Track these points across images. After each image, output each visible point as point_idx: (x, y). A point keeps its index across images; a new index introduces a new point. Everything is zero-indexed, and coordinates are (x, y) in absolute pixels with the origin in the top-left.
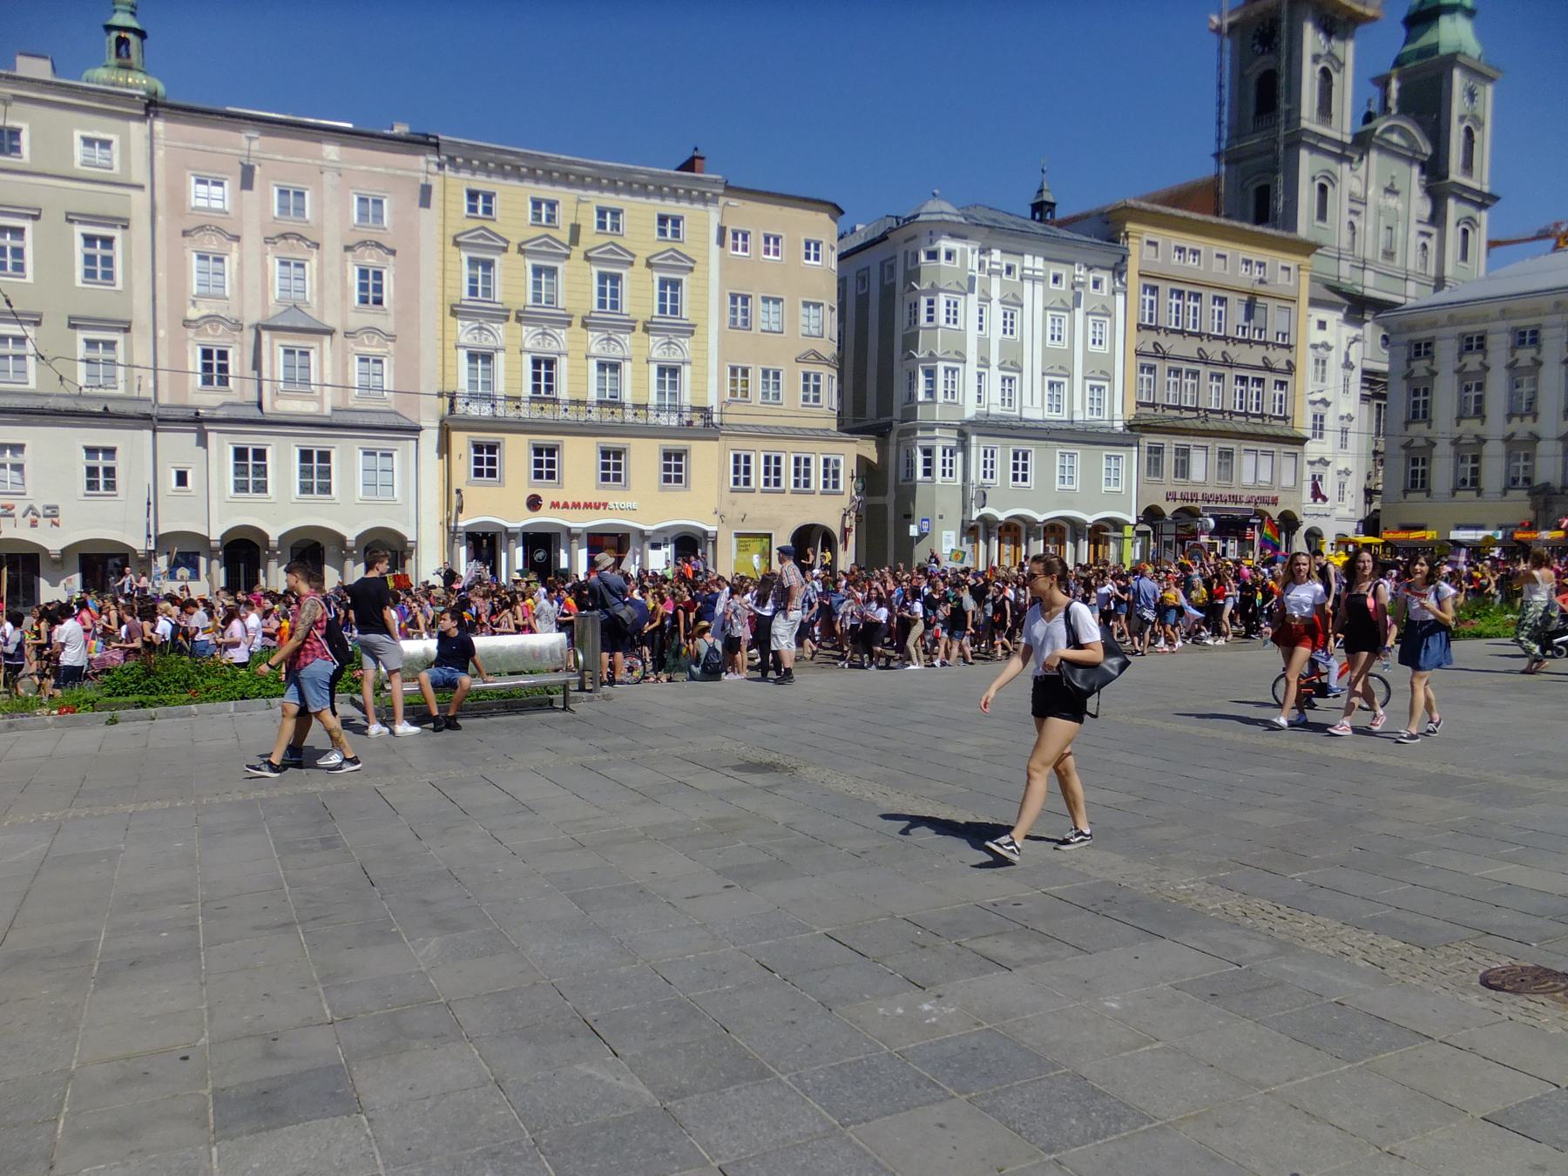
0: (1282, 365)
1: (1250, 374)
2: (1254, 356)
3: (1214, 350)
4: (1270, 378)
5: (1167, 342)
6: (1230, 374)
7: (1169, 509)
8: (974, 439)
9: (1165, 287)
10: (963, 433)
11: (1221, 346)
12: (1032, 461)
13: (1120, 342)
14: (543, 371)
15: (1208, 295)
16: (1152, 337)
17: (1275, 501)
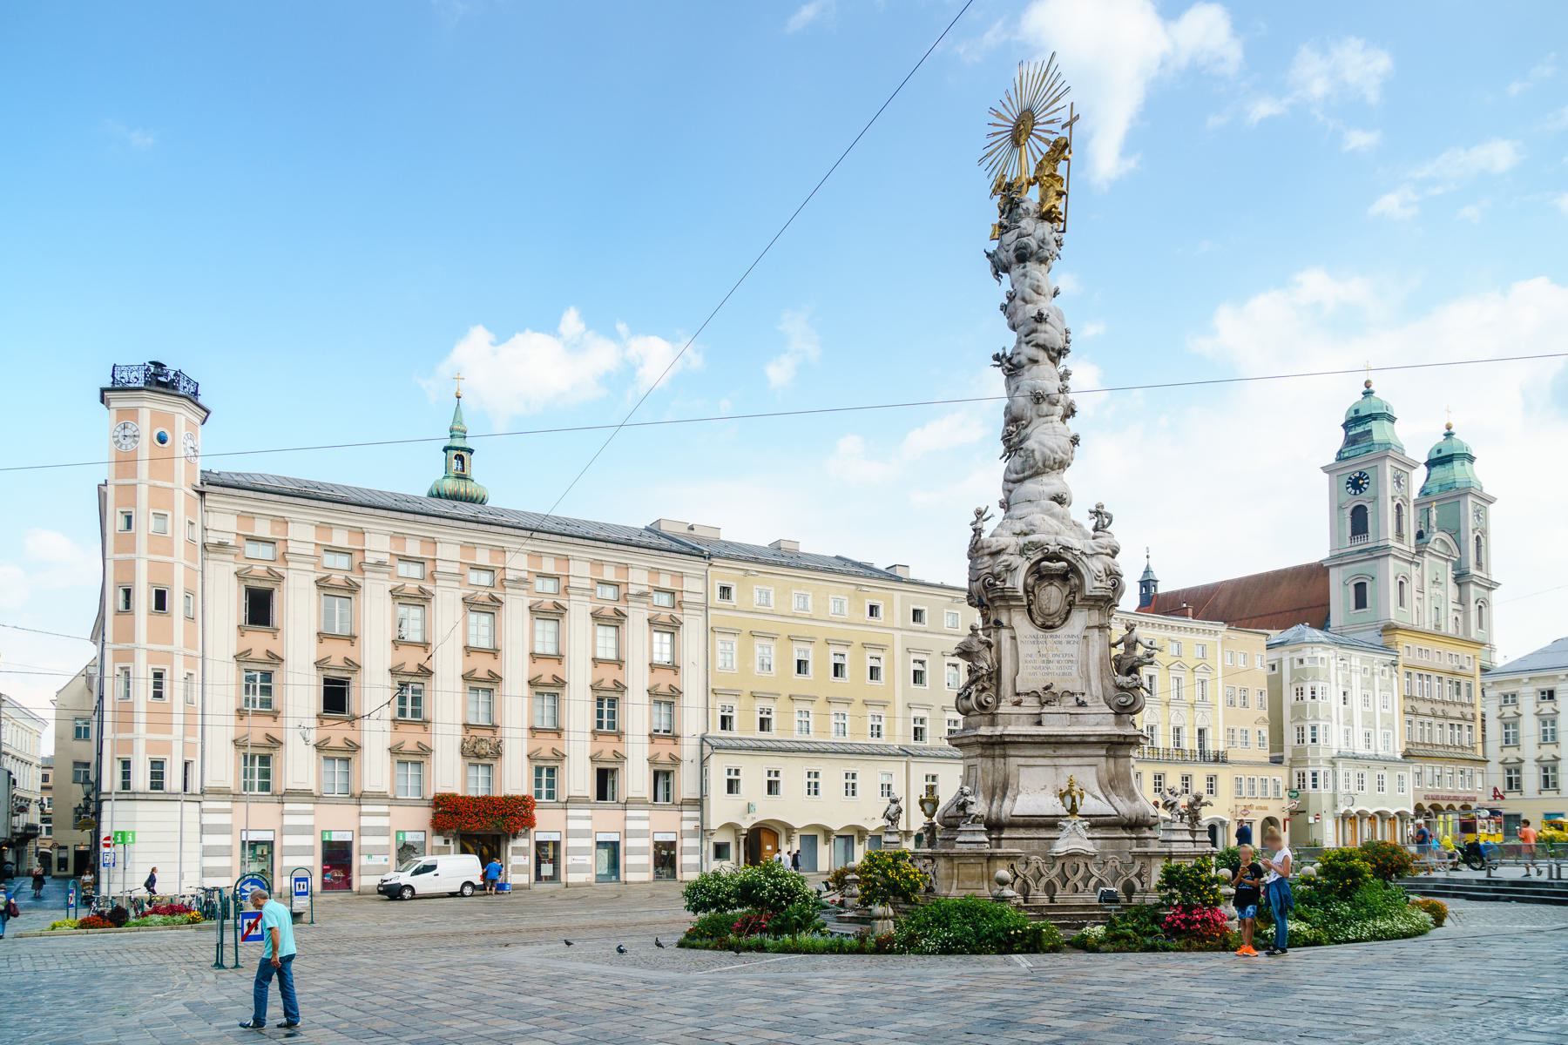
0: (1469, 717)
1: (1455, 722)
2: (1455, 712)
3: (1439, 708)
4: (1465, 724)
5: (1417, 705)
6: (1447, 723)
7: (1426, 805)
8: (1340, 764)
9: (1415, 672)
10: (1333, 762)
11: (1430, 705)
12: (1366, 779)
13: (1397, 705)
14: (606, 708)
15: (1434, 676)
16: (1410, 703)
17: (1474, 800)
